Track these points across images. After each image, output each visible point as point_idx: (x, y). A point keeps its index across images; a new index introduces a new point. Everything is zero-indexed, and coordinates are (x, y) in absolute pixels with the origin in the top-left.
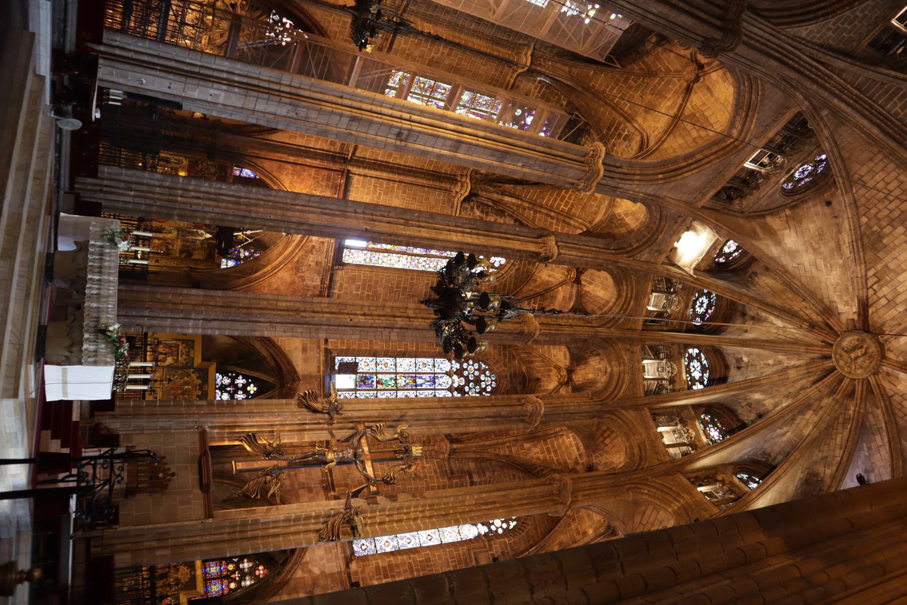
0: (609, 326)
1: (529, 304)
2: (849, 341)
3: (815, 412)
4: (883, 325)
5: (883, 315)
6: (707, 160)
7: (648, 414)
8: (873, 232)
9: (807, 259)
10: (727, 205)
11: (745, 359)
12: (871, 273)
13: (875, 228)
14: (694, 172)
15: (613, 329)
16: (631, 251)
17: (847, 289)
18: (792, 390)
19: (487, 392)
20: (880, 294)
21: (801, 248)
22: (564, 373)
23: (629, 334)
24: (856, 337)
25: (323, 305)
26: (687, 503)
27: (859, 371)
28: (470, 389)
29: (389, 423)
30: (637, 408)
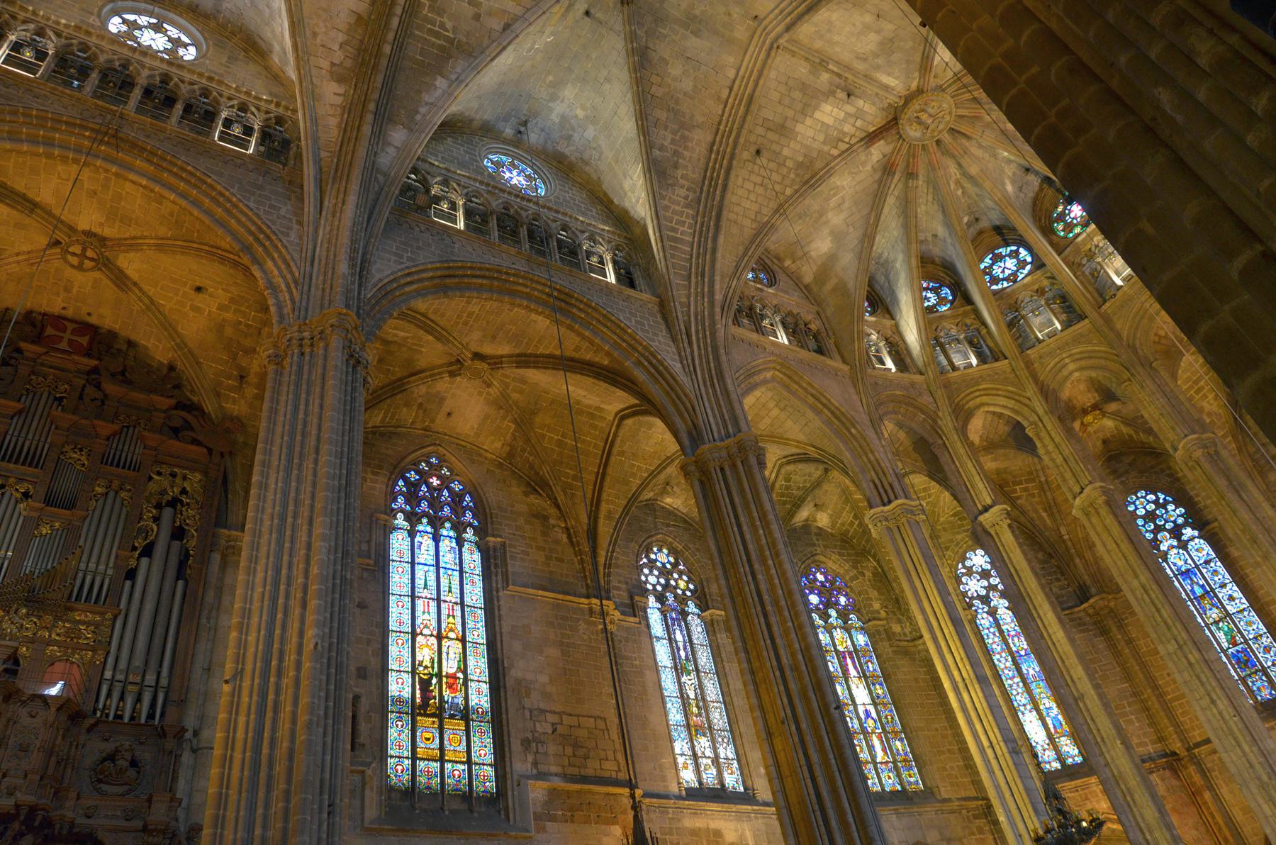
0: (1027, 401)
1: (1018, 498)
2: (913, 132)
7: (1107, 304)
8: (797, 175)
9: (836, 219)
10: (824, 335)
11: (966, 219)
12: (835, 152)
13: (792, 176)
15: (1029, 395)
16: (930, 417)
18: (987, 156)
19: (1158, 498)
20: (853, 130)
21: (826, 231)
22: (1089, 418)
23: (1023, 374)
24: (907, 128)
28: (1166, 521)
30: (1108, 320)
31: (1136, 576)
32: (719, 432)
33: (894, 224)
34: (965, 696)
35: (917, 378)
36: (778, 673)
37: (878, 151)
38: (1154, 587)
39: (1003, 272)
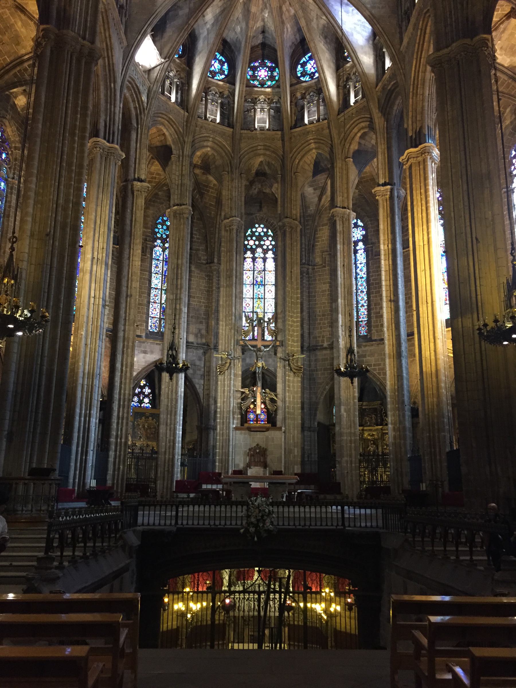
6: (108, 40)
7: (246, 131)
15: (186, 140)
18: (261, 7)
30: (240, 140)
32: (79, 30)
34: (95, 267)
36: (55, 205)
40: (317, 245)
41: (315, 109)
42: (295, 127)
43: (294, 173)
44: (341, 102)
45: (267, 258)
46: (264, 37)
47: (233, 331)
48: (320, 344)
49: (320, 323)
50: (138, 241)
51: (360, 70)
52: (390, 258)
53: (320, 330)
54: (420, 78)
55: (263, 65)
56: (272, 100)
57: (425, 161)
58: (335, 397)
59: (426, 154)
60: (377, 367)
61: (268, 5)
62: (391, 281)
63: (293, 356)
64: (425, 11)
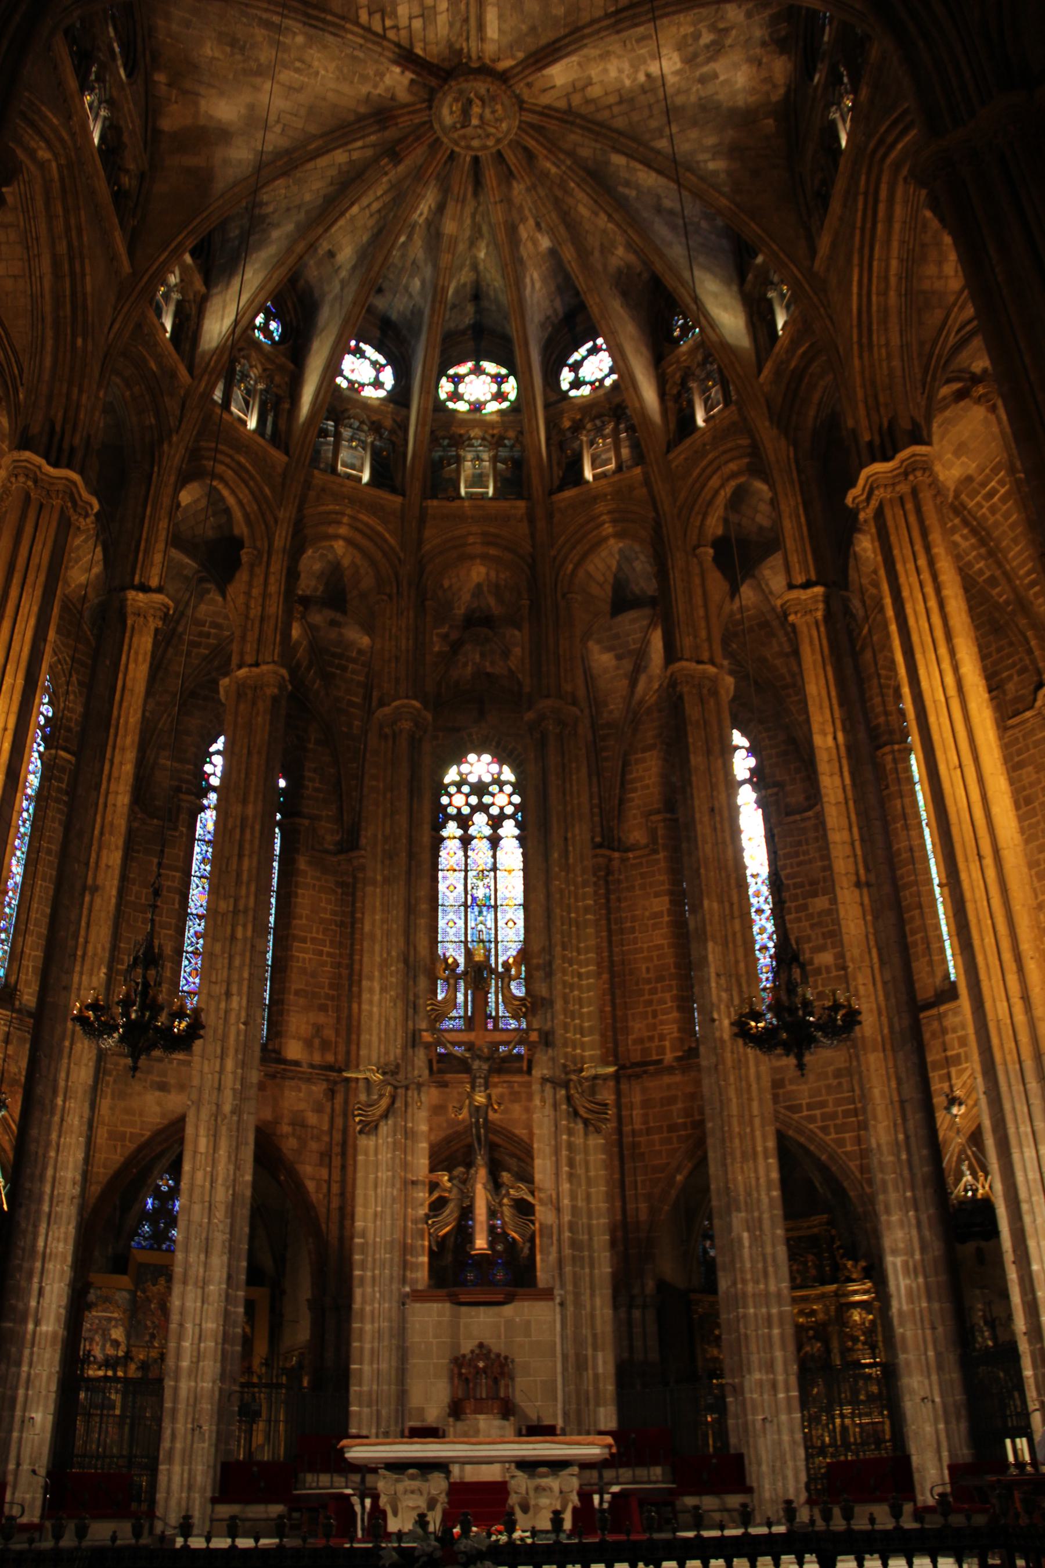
2: (448, 114)
3: (523, 220)
4: (450, 45)
5: (436, 34)
6: (74, 234)
7: (435, 503)
14: (88, 270)
15: (280, 515)
17: (355, 58)
18: (468, 233)
20: (403, 22)
24: (449, 99)
25: (206, 1069)
26: (609, 513)
27: (504, 126)
29: (411, 983)
30: (422, 520)
31: (245, 802)
33: (317, 185)
35: (183, 372)
37: (396, 80)
38: (258, 827)
39: (353, 371)
40: (632, 800)
41: (612, 454)
42: (561, 489)
43: (564, 595)
44: (672, 426)
45: (501, 838)
46: (479, 311)
47: (399, 1004)
48: (655, 1058)
49: (650, 1002)
50: (129, 740)
51: (713, 337)
52: (846, 769)
53: (651, 1020)
54: (874, 308)
55: (478, 371)
56: (502, 438)
57: (915, 492)
58: (713, 1187)
59: (919, 473)
60: (818, 1112)
61: (485, 229)
62: (855, 830)
63: (582, 1070)
64: (872, 145)
